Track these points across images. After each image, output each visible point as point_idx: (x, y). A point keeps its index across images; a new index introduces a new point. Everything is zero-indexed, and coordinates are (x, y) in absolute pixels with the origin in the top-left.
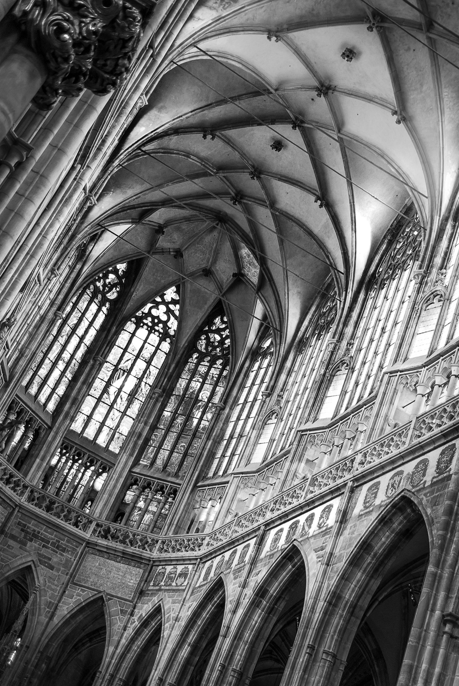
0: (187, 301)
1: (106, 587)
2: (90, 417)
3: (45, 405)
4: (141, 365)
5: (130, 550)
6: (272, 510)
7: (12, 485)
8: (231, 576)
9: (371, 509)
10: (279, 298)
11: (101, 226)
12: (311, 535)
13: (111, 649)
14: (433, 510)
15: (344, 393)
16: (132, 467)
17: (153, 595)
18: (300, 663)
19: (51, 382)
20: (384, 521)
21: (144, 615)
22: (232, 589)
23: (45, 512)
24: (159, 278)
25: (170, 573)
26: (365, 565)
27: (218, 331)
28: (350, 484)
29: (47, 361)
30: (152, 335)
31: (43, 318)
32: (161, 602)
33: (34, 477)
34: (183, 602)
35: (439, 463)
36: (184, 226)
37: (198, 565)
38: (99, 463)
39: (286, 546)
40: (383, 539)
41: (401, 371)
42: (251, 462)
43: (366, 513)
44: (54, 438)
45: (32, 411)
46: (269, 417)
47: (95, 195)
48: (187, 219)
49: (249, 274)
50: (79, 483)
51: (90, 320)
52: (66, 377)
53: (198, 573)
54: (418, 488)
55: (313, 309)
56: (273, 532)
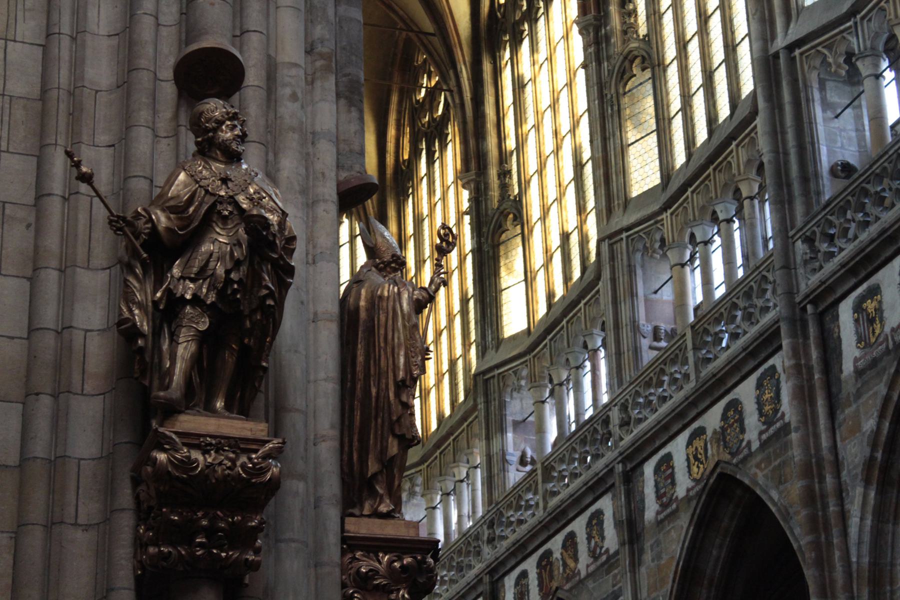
6: (491, 541)
9: (674, 506)
12: (583, 574)
14: (780, 493)
20: (704, 524)
28: (619, 468)
35: (760, 404)
40: (715, 552)
41: (628, 229)
54: (741, 456)
55: (395, 99)
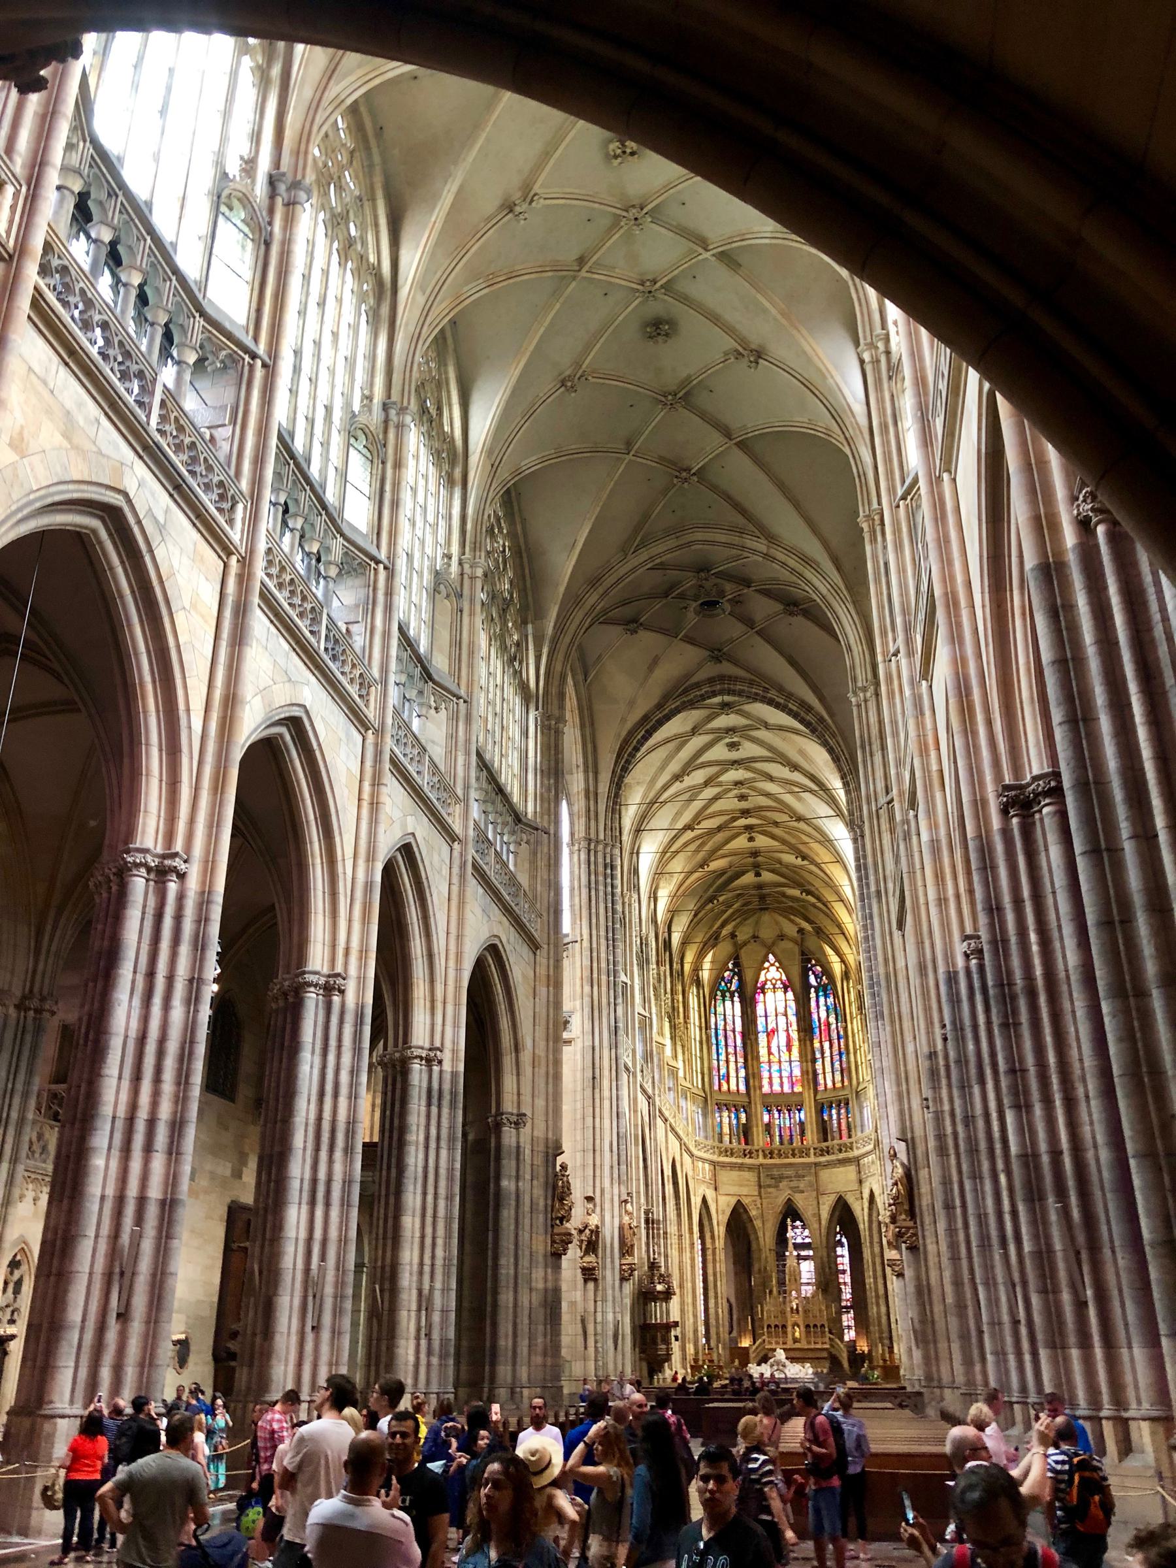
1: (841, 1188)
2: (770, 1078)
4: (782, 1019)
5: (841, 1156)
13: (861, 1226)
19: (733, 1073)
31: (701, 1042)
33: (760, 1139)
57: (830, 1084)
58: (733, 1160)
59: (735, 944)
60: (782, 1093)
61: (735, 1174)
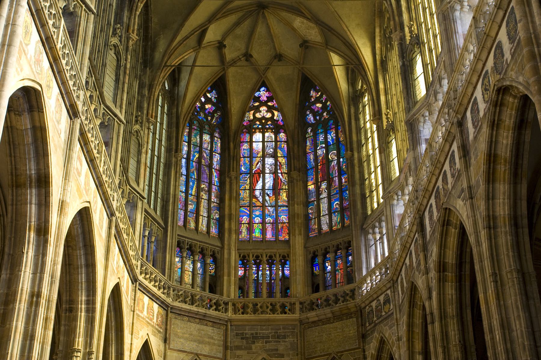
0: (278, 90)
3: (208, 232)
4: (270, 161)
7: (214, 307)
8: (417, 273)
10: (345, 39)
11: (168, 66)
12: (450, 189)
15: (425, 65)
16: (305, 244)
17: (372, 332)
18: (491, 294)
19: (203, 212)
21: (373, 352)
22: (420, 282)
23: (253, 315)
24: (245, 86)
25: (377, 307)
26: (502, 176)
27: (318, 100)
29: (190, 198)
30: (267, 134)
31: (168, 166)
32: (381, 334)
34: (397, 322)
36: (238, 31)
37: (393, 286)
38: (278, 255)
39: (439, 215)
42: (393, 179)
43: (478, 131)
44: (229, 254)
45: (200, 242)
46: (388, 135)
47: (133, 33)
48: (237, 24)
49: (312, 37)
50: (271, 280)
51: (209, 149)
52: (214, 202)
53: (396, 293)
56: (427, 214)
57: (325, 228)
58: (194, 308)
59: (222, 58)
60: (263, 240)
61: (194, 327)
